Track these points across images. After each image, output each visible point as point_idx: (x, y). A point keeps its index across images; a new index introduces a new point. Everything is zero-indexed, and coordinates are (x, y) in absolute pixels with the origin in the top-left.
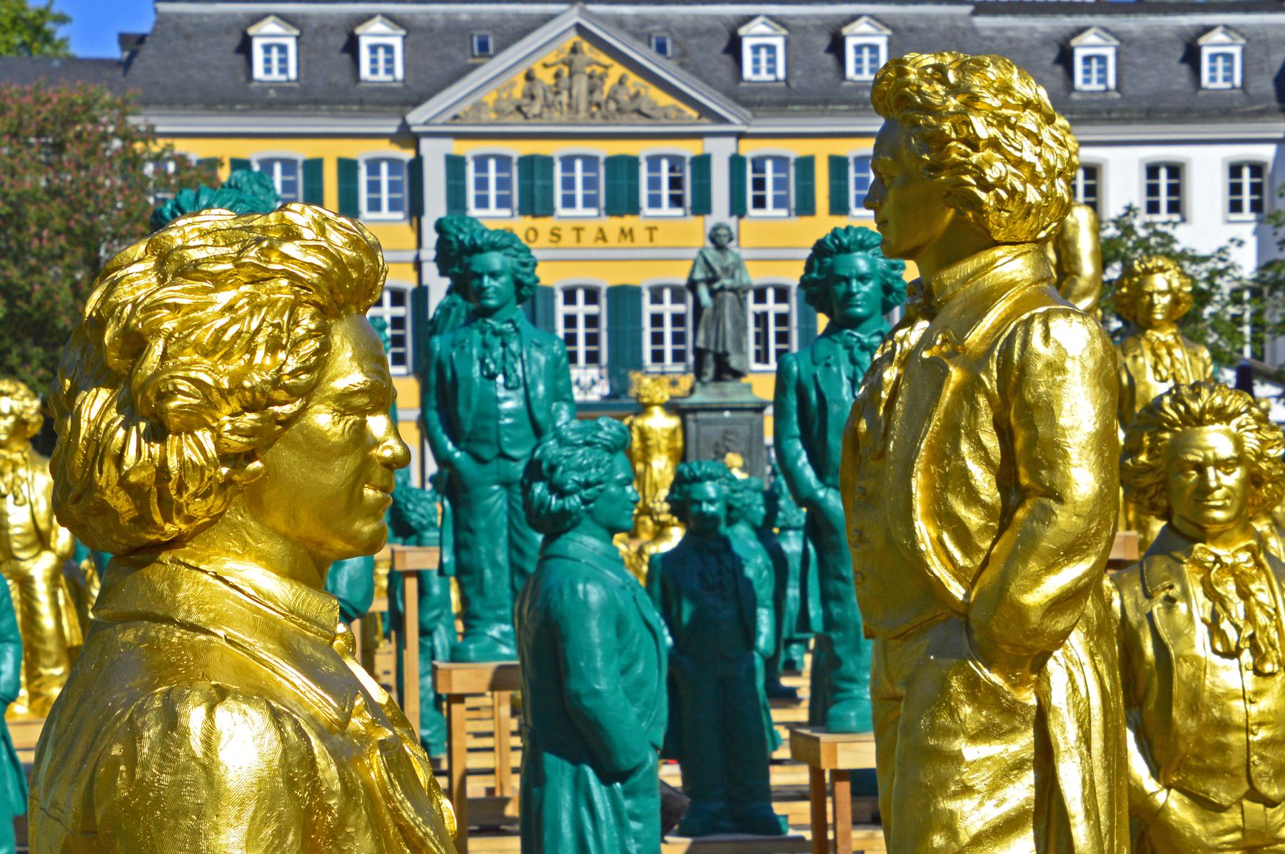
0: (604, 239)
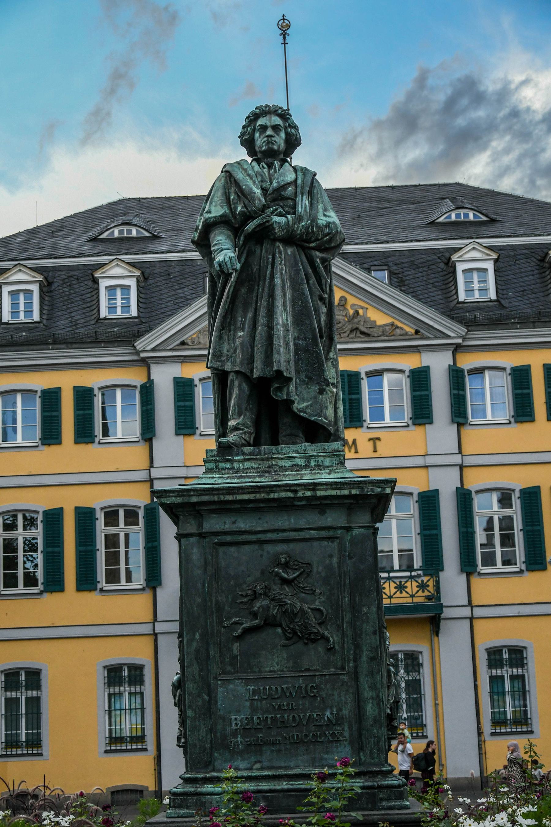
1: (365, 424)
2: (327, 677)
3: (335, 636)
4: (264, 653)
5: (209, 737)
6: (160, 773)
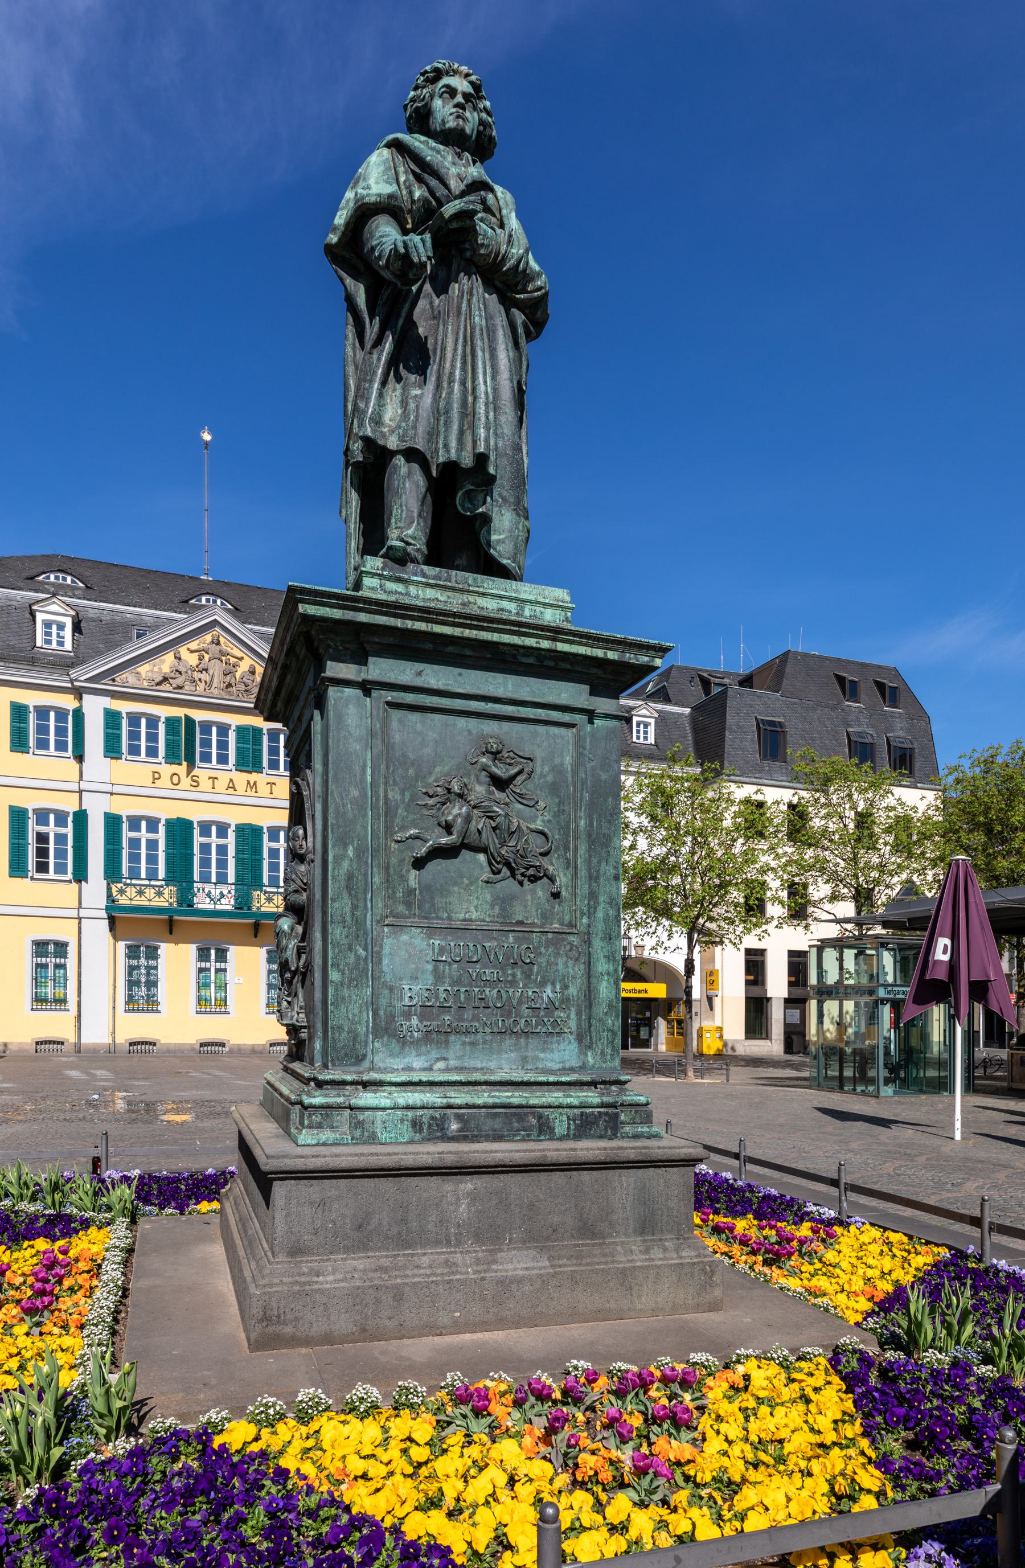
0: (234, 788)
1: (264, 771)
2: (550, 936)
3: (562, 875)
4: (456, 889)
5: (365, 1016)
6: (79, 1029)
